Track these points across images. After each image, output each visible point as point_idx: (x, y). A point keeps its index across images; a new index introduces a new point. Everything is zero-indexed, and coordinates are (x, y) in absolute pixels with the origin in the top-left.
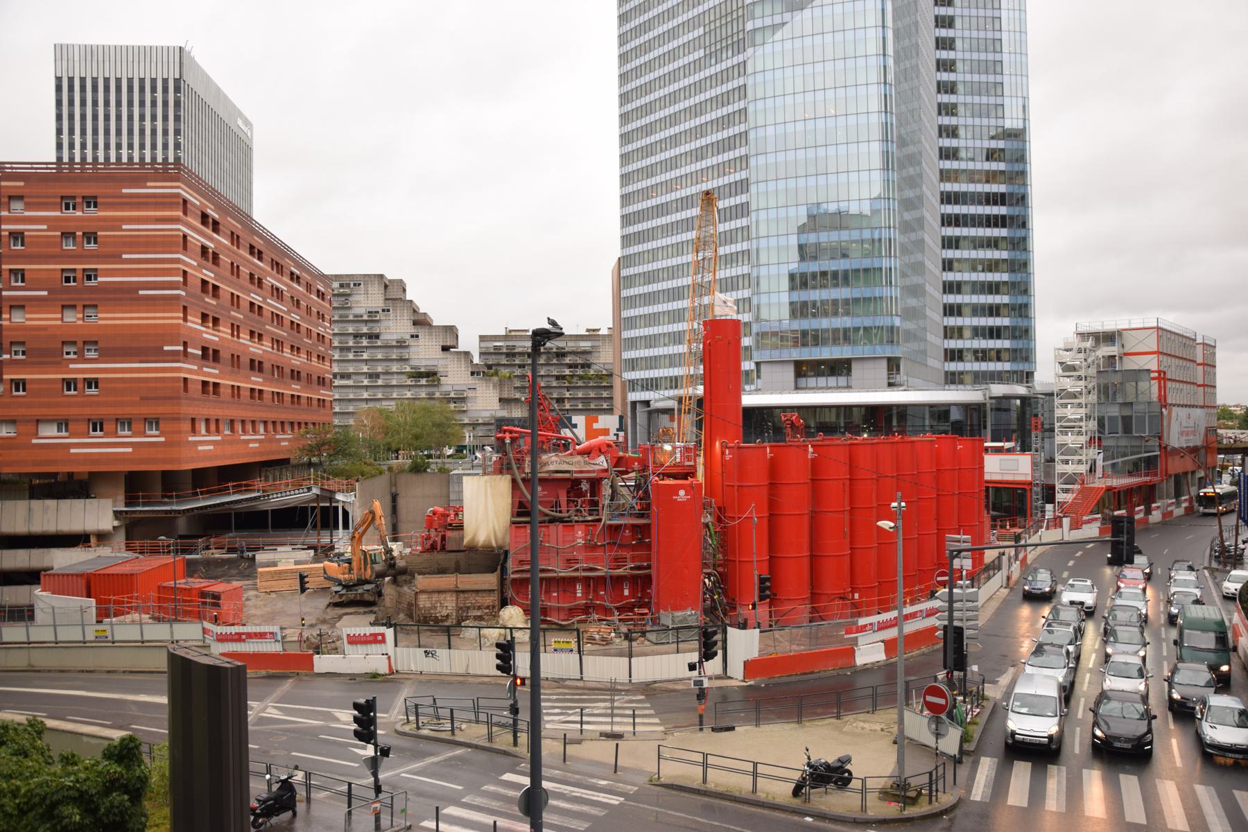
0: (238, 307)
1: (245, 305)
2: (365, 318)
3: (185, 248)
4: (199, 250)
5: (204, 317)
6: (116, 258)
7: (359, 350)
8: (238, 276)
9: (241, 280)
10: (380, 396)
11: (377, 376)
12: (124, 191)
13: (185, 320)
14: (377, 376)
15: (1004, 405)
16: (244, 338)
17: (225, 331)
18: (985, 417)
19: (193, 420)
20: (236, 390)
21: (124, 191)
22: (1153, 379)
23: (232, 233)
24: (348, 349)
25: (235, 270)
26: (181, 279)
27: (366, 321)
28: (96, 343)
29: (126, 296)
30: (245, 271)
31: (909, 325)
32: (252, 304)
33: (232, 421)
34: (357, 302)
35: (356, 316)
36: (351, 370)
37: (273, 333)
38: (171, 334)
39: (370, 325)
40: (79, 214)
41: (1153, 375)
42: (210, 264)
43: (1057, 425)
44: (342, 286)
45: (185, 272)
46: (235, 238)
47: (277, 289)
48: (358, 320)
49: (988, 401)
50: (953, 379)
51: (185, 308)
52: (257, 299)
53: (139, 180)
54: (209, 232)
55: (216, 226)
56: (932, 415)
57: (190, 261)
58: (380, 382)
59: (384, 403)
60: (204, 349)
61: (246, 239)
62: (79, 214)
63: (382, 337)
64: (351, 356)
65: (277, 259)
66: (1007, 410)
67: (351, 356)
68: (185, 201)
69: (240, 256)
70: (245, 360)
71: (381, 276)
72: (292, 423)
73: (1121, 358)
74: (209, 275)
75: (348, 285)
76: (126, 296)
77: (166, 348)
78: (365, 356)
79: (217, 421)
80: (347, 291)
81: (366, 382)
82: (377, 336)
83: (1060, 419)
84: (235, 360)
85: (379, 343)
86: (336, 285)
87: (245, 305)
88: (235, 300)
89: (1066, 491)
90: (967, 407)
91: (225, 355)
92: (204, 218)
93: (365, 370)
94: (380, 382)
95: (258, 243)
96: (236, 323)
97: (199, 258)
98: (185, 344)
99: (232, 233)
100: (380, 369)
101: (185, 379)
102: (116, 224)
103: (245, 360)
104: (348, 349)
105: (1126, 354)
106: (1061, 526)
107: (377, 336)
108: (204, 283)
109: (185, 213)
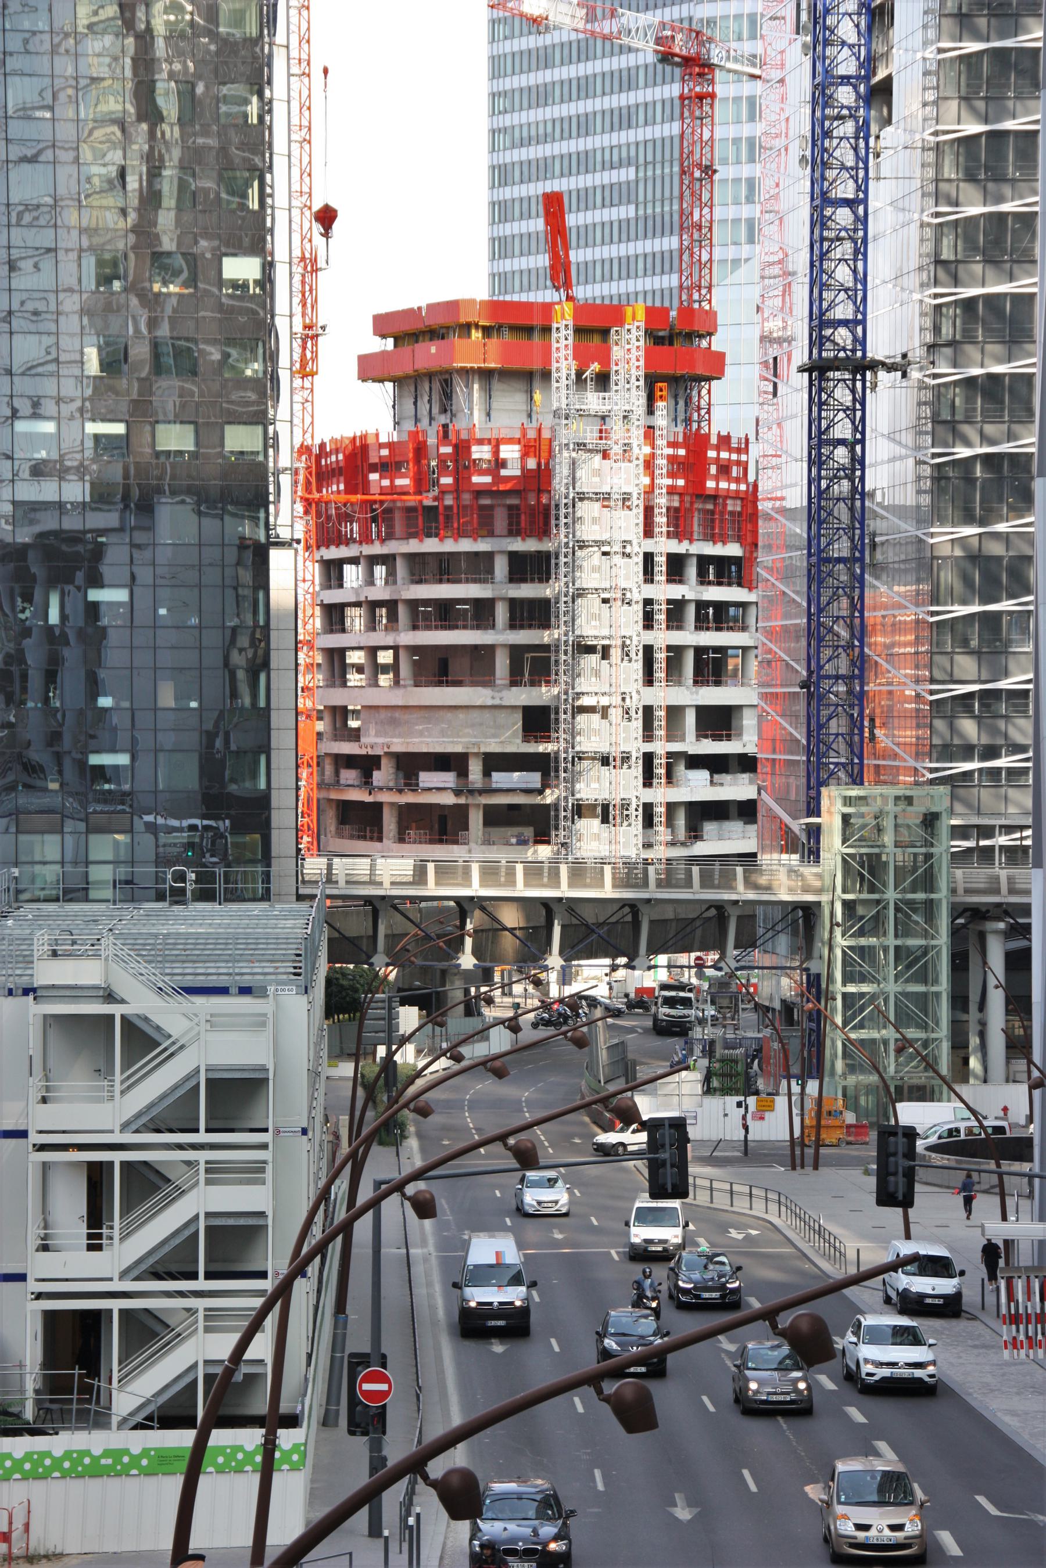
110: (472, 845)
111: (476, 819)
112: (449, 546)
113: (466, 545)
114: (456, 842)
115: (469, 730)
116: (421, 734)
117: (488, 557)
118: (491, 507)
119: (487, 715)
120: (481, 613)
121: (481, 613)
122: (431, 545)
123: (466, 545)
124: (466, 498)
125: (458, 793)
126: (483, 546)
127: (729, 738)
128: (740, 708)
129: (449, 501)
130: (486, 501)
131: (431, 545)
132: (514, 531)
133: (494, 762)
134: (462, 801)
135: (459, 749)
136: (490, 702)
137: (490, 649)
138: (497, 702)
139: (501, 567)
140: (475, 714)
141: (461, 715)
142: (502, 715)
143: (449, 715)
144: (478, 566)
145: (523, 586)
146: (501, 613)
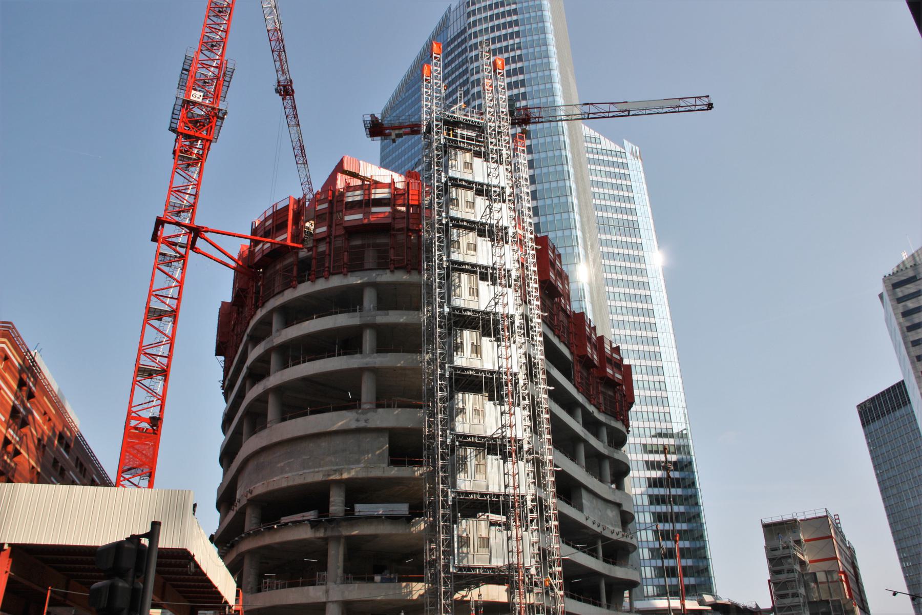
110: (331, 585)
111: (336, 557)
112: (321, 285)
113: (336, 281)
114: (313, 584)
116: (282, 471)
117: (358, 290)
118: (363, 246)
119: (351, 440)
120: (348, 342)
121: (348, 342)
122: (305, 289)
123: (336, 281)
124: (339, 243)
125: (314, 525)
126: (355, 279)
128: (579, 486)
129: (322, 248)
130: (358, 242)
131: (305, 289)
132: (383, 264)
133: (358, 491)
134: (321, 534)
135: (319, 478)
136: (354, 425)
138: (362, 424)
139: (369, 299)
140: (338, 441)
141: (324, 443)
142: (367, 439)
143: (311, 445)
144: (347, 300)
145: (391, 312)
146: (368, 339)
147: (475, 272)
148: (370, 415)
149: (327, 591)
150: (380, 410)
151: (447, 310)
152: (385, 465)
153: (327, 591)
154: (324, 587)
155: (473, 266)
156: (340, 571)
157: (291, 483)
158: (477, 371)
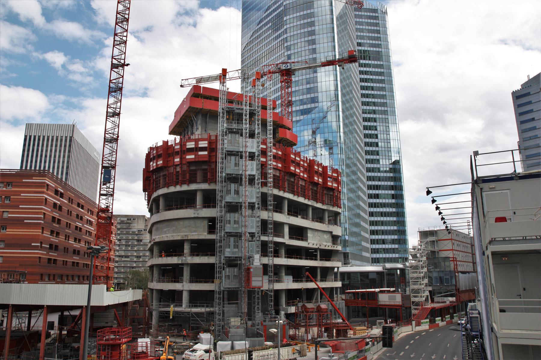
0: (70, 227)
1: (73, 227)
2: (137, 233)
3: (46, 203)
4: (52, 205)
5: (52, 232)
6: (17, 207)
7: (133, 246)
8: (71, 215)
9: (72, 217)
10: (141, 265)
11: (140, 257)
12: (24, 180)
13: (43, 233)
14: (140, 257)
15: (392, 272)
16: (71, 242)
17: (62, 238)
18: (384, 277)
19: (42, 275)
20: (65, 263)
21: (24, 180)
22: (451, 261)
23: (70, 198)
24: (129, 246)
25: (69, 213)
26: (42, 216)
27: (137, 234)
28: (4, 241)
29: (19, 222)
30: (74, 213)
31: (353, 239)
32: (76, 227)
33: (62, 276)
34: (134, 226)
35: (133, 232)
36: (129, 254)
37: (85, 239)
38: (35, 238)
39: (138, 236)
40: (5, 189)
41: (451, 259)
42: (57, 210)
43: (410, 281)
44: (128, 219)
45: (44, 214)
46: (70, 200)
47: (90, 221)
48: (134, 233)
49: (385, 271)
50: (375, 261)
51: (43, 228)
52: (79, 224)
53: (30, 176)
54: (58, 197)
55: (62, 195)
56: (361, 276)
57: (47, 209)
58: (141, 260)
59: (137, 269)
60: (51, 245)
61: (76, 200)
62: (5, 189)
63: (143, 241)
64: (130, 249)
65: (90, 208)
66: (393, 275)
67: (130, 249)
68: (48, 185)
69: (73, 208)
70: (71, 250)
71: (144, 216)
72: (79, 277)
73: (438, 252)
74: (56, 215)
75: (130, 219)
76: (19, 222)
77: (33, 244)
78: (135, 249)
79: (54, 275)
80: (130, 222)
81: (135, 260)
82: (141, 241)
83: (412, 278)
84: (66, 250)
85: (142, 244)
86: (126, 219)
87: (73, 227)
88: (68, 225)
89: (415, 309)
90: (378, 273)
91: (61, 247)
92: (56, 192)
93: (135, 254)
94: (141, 260)
95: (82, 202)
96: (68, 235)
97: (52, 208)
98: (41, 243)
99: (70, 198)
100: (141, 254)
101: (40, 257)
102: (18, 193)
103: (71, 250)
104: (129, 246)
105: (440, 251)
106: (411, 325)
107: (141, 241)
108: (54, 218)
109: (47, 190)
110: (184, 283)
114: (178, 282)
115: (184, 229)
116: (166, 233)
119: (192, 222)
127: (302, 240)
128: (306, 229)
135: (179, 238)
136: (193, 216)
137: (194, 192)
138: (196, 215)
141: (181, 223)
142: (198, 222)
143: (176, 223)
147: (238, 155)
148: (199, 211)
149: (183, 286)
150: (204, 209)
151: (224, 175)
152: (206, 234)
153: (183, 286)
154: (181, 284)
155: (237, 152)
156: (188, 278)
157: (168, 239)
158: (237, 203)
